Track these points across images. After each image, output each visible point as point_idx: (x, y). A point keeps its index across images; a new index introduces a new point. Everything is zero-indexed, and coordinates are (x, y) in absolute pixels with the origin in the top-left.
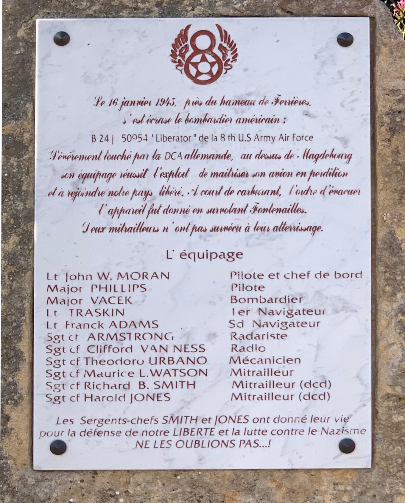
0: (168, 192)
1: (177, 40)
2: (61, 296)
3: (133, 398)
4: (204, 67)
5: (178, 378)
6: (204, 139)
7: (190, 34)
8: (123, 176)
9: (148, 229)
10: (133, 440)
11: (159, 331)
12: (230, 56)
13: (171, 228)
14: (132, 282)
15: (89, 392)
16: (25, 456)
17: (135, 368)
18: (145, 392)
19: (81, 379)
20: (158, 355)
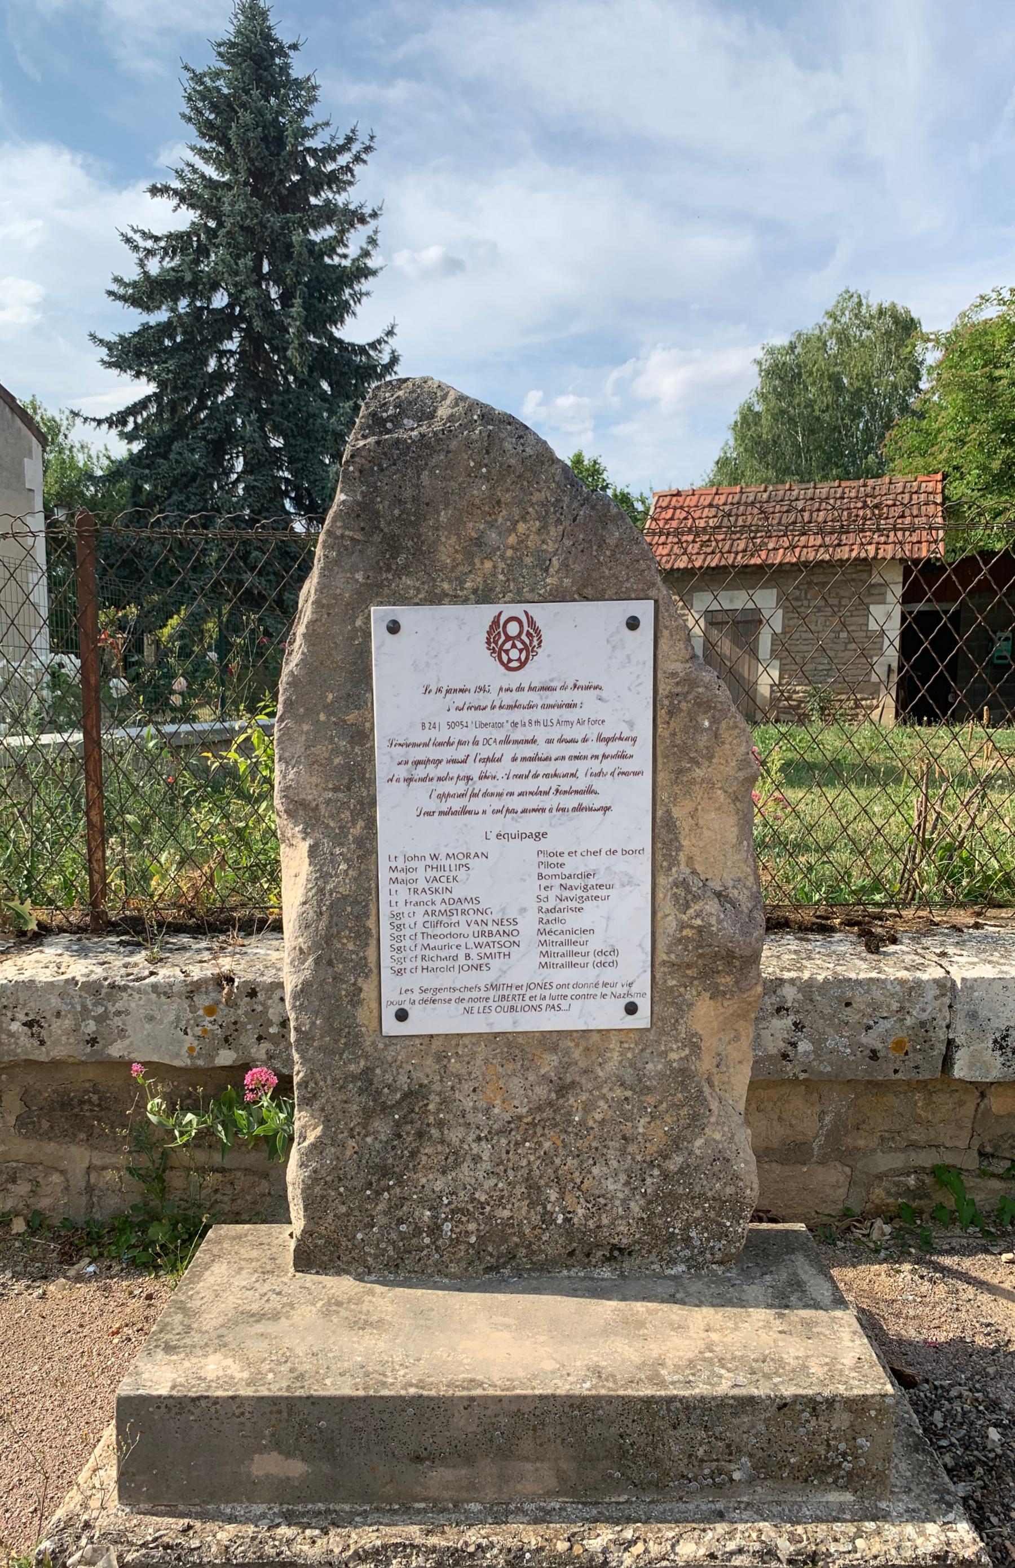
0: (486, 777)
1: (491, 627)
2: (401, 876)
3: (461, 968)
4: (514, 654)
5: (496, 950)
6: (515, 725)
7: (502, 622)
8: (448, 762)
9: (470, 812)
10: (461, 1006)
11: (480, 907)
12: (535, 643)
13: (489, 811)
14: (458, 862)
15: (425, 964)
16: (374, 1024)
17: (461, 941)
18: (470, 962)
19: (419, 952)
20: (480, 929)
